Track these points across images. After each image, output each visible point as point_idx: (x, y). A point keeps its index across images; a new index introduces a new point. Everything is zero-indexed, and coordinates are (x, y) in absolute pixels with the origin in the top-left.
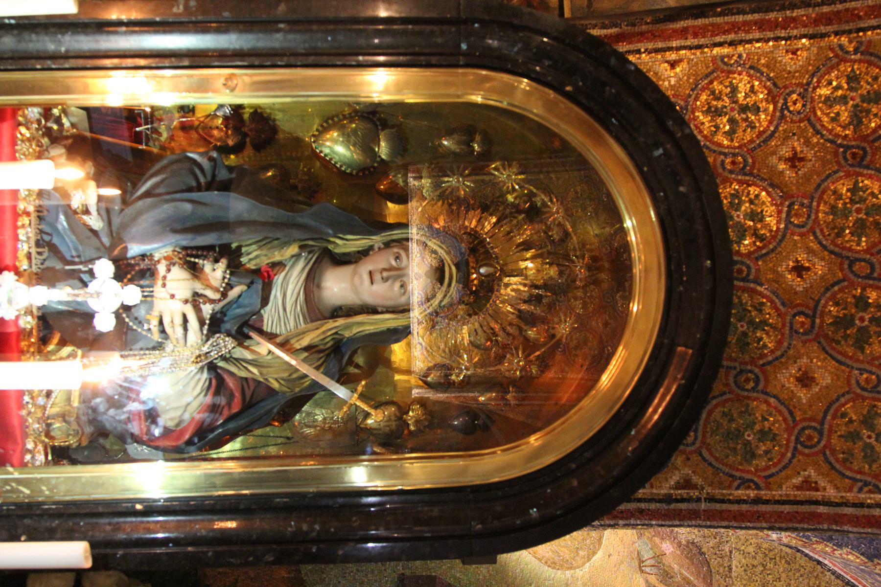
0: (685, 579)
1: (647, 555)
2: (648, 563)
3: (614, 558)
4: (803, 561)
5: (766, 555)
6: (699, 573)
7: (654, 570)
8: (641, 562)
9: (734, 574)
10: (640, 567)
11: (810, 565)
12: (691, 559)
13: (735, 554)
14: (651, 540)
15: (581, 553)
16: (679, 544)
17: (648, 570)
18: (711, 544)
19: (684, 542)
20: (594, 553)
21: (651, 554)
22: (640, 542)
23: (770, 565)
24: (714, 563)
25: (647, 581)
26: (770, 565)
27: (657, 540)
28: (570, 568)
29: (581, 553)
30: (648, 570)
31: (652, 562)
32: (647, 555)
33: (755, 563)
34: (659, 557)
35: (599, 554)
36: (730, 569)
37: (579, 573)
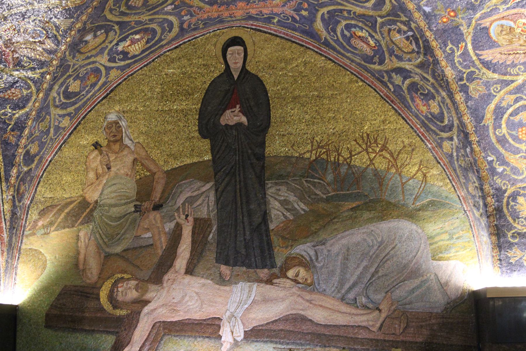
0: (53, 216)
1: (43, 231)
2: (46, 231)
3: (43, 244)
4: (49, 168)
5: (46, 183)
6: (51, 211)
7: (49, 228)
8: (45, 234)
9: (53, 196)
10: (47, 234)
11: (51, 164)
12: (45, 214)
13: (45, 196)
14: (37, 230)
15: (40, 257)
16: (40, 218)
17: (48, 231)
18: (40, 206)
19: (39, 217)
20: (41, 252)
21: (42, 230)
22: (38, 235)
23: (50, 182)
24: (48, 204)
25: (53, 231)
26: (50, 182)
27: (37, 227)
28: (46, 261)
29: (40, 257)
30: (48, 231)
31: (46, 229)
32: (43, 231)
33: (49, 188)
34: (44, 227)
35: (41, 250)
36: (51, 198)
37: (48, 258)
